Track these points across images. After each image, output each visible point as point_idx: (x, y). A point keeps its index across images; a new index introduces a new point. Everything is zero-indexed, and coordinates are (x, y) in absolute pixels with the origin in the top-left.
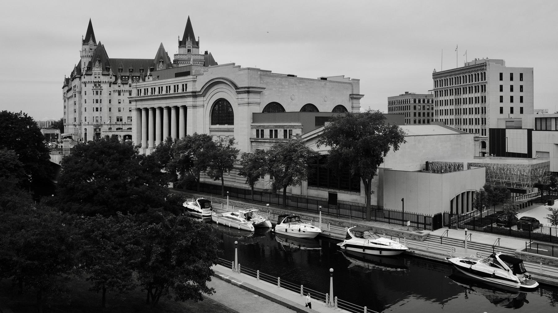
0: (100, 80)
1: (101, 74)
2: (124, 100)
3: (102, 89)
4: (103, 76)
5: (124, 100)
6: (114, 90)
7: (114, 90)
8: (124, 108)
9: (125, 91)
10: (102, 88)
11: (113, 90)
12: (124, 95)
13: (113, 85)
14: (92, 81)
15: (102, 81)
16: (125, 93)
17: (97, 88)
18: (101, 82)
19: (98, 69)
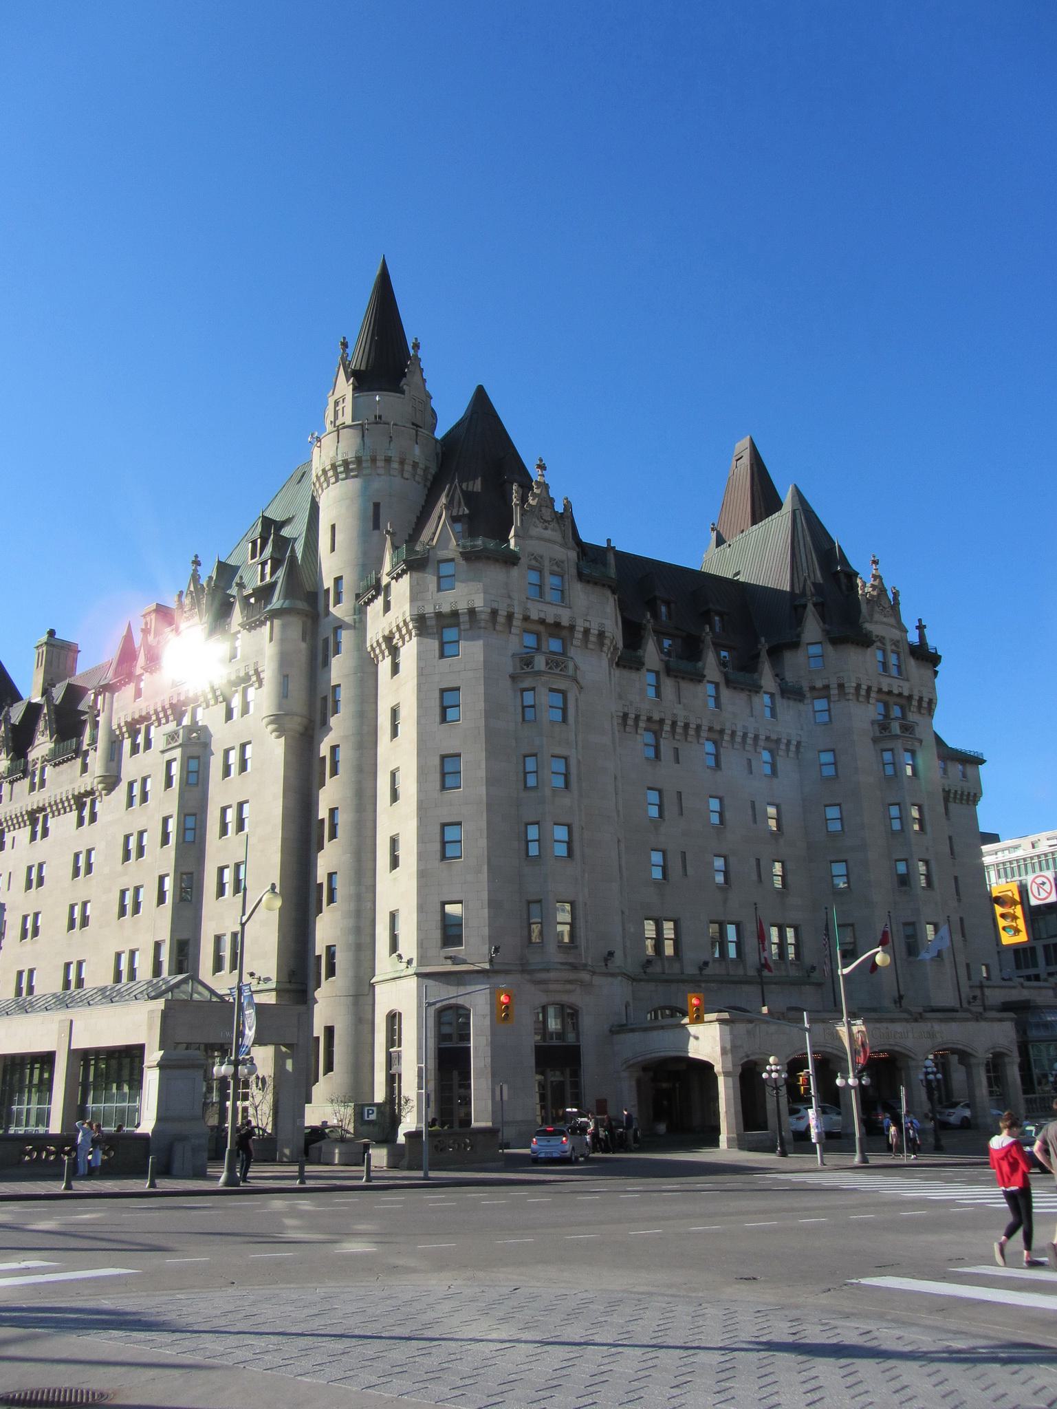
1: (573, 571)
2: (679, 794)
5: (679, 794)
7: (625, 716)
12: (677, 761)
15: (580, 626)
18: (572, 628)
19: (548, 534)
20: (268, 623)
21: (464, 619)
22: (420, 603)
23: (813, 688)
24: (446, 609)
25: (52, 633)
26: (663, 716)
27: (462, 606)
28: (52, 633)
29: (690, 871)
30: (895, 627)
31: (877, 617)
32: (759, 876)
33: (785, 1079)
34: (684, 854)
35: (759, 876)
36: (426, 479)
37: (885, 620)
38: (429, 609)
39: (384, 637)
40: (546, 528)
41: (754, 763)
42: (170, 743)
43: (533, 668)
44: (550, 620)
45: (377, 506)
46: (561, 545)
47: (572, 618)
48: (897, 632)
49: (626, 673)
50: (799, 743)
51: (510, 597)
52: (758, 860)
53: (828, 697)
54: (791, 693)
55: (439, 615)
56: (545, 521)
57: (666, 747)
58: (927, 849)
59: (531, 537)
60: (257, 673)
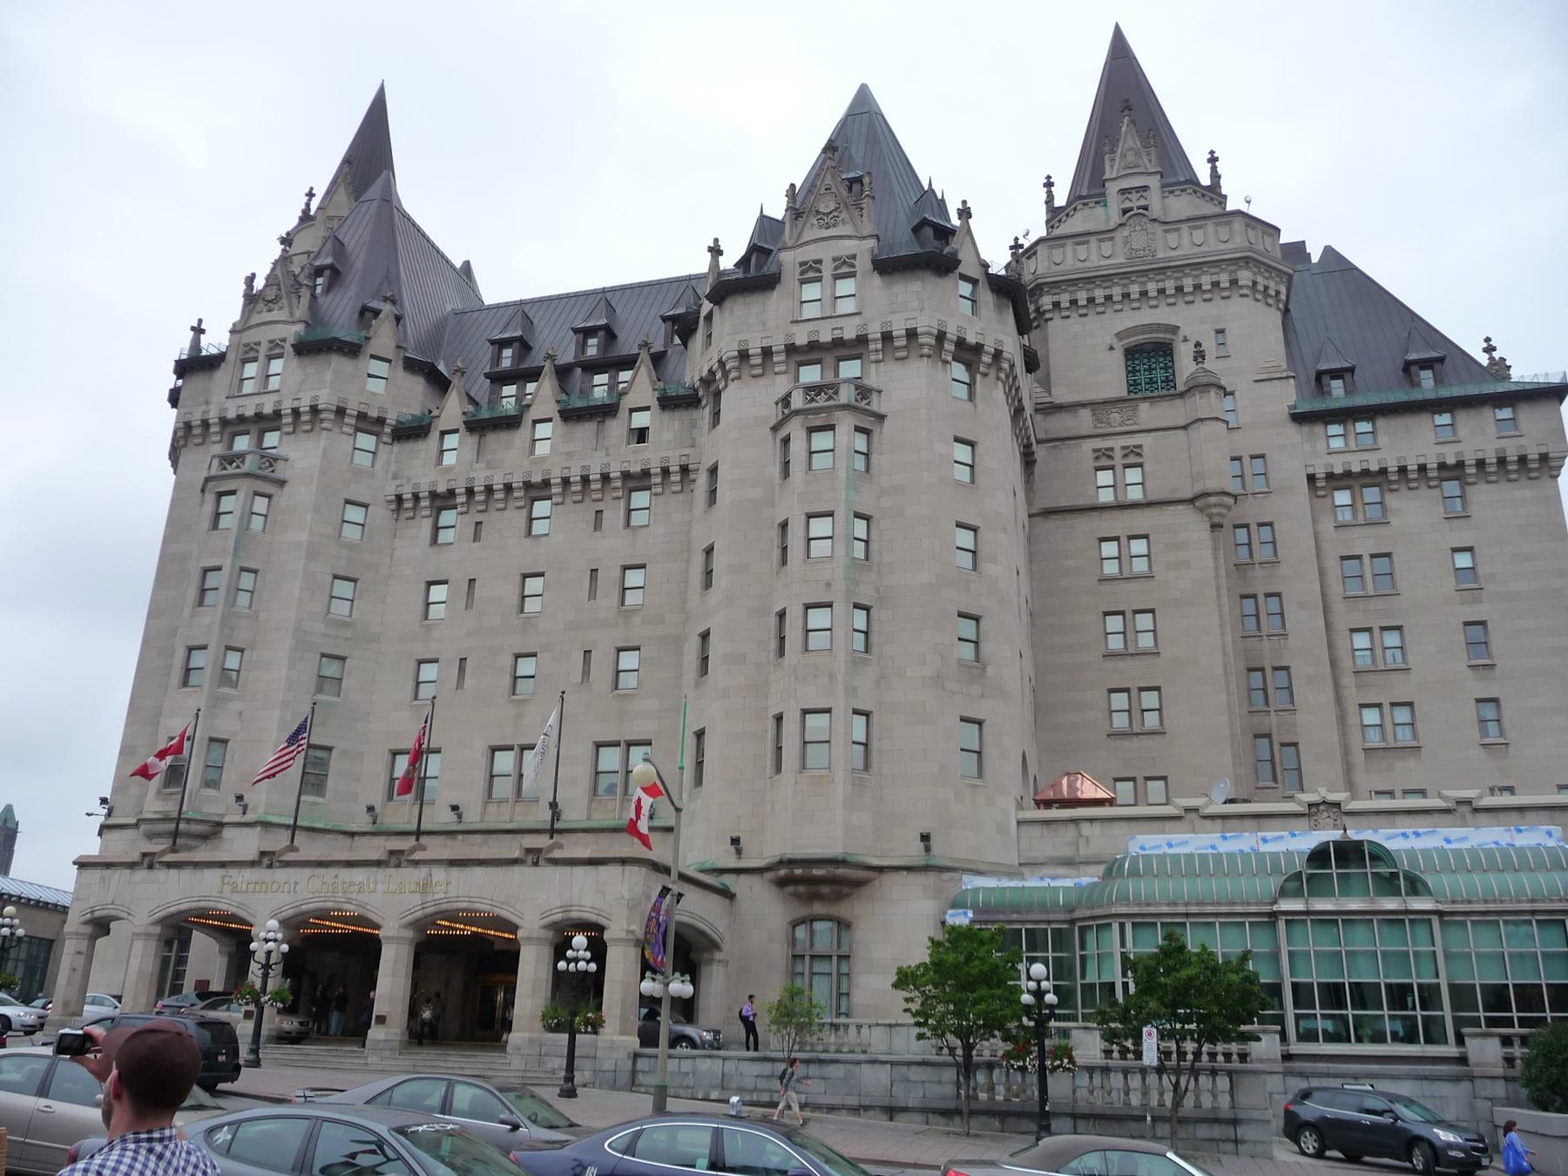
0: (274, 397)
3: (282, 483)
4: (307, 360)
5: (472, 581)
6: (399, 499)
7: (399, 499)
8: (463, 660)
9: (489, 490)
10: (281, 471)
11: (391, 491)
12: (476, 538)
13: (396, 447)
14: (213, 417)
15: (286, 408)
16: (493, 520)
19: (276, 315)
26: (453, 485)
29: (469, 681)
30: (850, 237)
31: (807, 236)
32: (586, 673)
33: (284, 954)
34: (463, 660)
35: (586, 673)
40: (269, 311)
41: (605, 514)
44: (250, 412)
46: (284, 322)
47: (279, 402)
49: (409, 447)
50: (685, 470)
51: (207, 403)
52: (587, 652)
56: (270, 301)
58: (828, 585)
59: (250, 328)
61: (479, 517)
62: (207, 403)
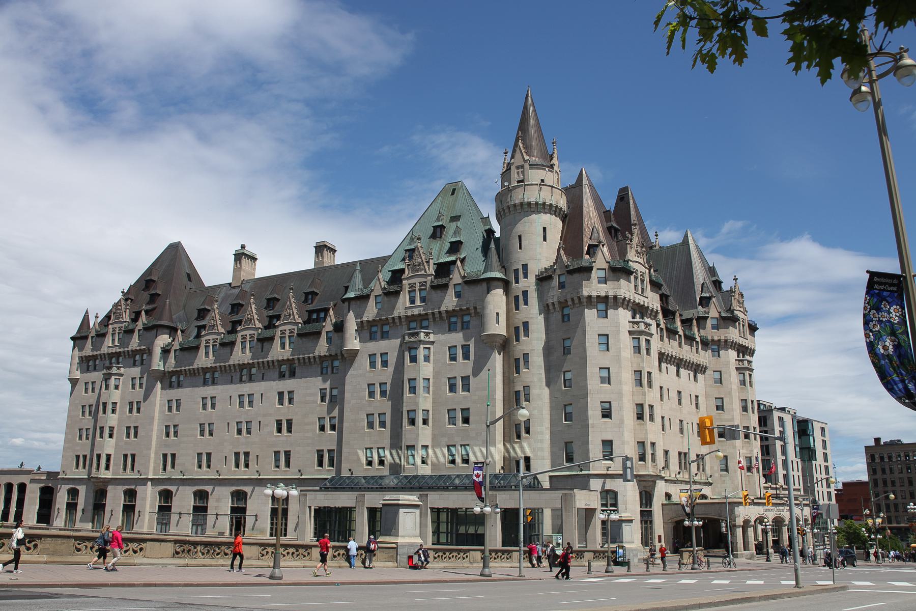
17: (647, 330)
19: (639, 260)
20: (484, 285)
21: (611, 301)
22: (588, 289)
23: (713, 340)
24: (603, 294)
25: (243, 247)
27: (611, 294)
28: (243, 247)
36: (563, 216)
37: (740, 309)
38: (594, 294)
39: (560, 302)
42: (411, 338)
43: (638, 327)
45: (545, 229)
48: (743, 315)
51: (629, 291)
53: (719, 346)
54: (705, 344)
55: (598, 297)
56: (639, 253)
57: (664, 365)
60: (475, 308)
61: (667, 365)
62: (629, 291)
